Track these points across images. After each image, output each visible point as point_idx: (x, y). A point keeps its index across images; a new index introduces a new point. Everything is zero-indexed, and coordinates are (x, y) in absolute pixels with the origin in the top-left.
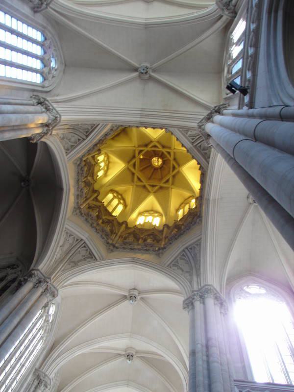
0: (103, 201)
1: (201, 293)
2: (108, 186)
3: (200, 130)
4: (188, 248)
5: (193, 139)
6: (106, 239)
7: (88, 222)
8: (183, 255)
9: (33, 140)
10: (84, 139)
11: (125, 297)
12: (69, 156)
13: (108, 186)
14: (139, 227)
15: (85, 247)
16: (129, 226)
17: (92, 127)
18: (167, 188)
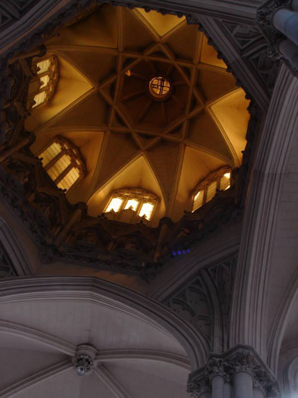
0: (40, 157)
1: (227, 361)
2: (52, 126)
3: (261, 22)
4: (209, 270)
5: (243, 43)
6: (40, 234)
7: (7, 195)
8: (198, 282)
10: (15, 19)
11: (66, 360)
13: (52, 126)
14: (110, 218)
16: (90, 213)
18: (176, 145)
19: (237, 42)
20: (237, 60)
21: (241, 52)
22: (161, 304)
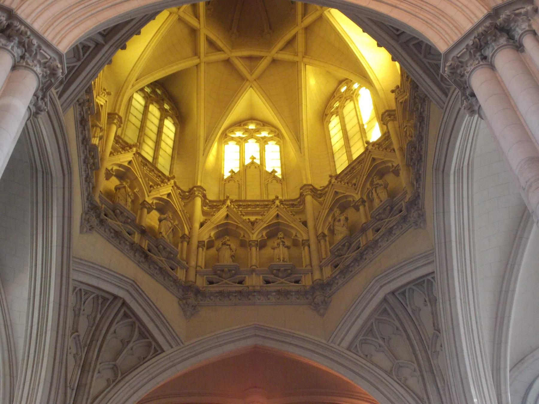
10: (124, 303)
12: (165, 346)
15: (404, 293)
22: (450, 95)
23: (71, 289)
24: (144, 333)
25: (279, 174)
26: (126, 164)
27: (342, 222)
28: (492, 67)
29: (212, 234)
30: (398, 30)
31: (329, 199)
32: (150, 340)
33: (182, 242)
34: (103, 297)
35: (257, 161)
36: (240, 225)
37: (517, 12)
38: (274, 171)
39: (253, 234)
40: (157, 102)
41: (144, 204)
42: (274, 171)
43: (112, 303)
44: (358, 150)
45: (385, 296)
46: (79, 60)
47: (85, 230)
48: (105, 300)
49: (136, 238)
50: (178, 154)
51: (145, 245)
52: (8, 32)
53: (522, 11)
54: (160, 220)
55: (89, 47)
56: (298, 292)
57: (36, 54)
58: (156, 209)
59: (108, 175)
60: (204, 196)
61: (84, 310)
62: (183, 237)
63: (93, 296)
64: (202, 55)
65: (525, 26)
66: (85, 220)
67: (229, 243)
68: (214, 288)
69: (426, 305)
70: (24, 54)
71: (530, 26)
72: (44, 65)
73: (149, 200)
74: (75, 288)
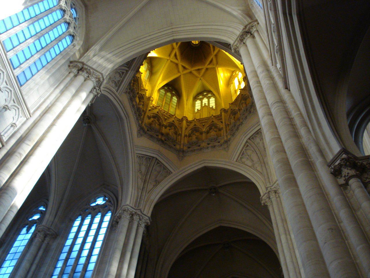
5: (123, 73)
9: (147, 223)
10: (156, 159)
17: (142, 157)
19: (124, 75)
20: (132, 71)
21: (127, 71)
23: (136, 157)
24: (165, 168)
25: (214, 107)
26: (156, 113)
27: (232, 118)
28: (246, 46)
29: (190, 132)
30: (227, 44)
31: (229, 112)
32: (167, 170)
33: (179, 136)
34: (148, 158)
35: (207, 105)
36: (200, 127)
37: (253, 25)
38: (213, 107)
39: (204, 129)
40: (170, 92)
41: (163, 125)
42: (213, 107)
43: (152, 160)
44: (238, 93)
45: (247, 141)
46: (121, 77)
47: (139, 136)
48: (150, 159)
49: (160, 137)
50: (178, 107)
51: (163, 138)
52: (82, 70)
53: (254, 25)
54: (169, 130)
55: (124, 72)
56: (218, 146)
57: (93, 75)
58: (168, 126)
59: (149, 118)
60: (187, 119)
61: (142, 163)
62: (179, 135)
63: (145, 158)
64: (181, 72)
65: (255, 29)
66: (139, 132)
67: (195, 134)
68: (190, 149)
69: (261, 141)
70: (89, 76)
71: (256, 29)
72: (96, 78)
73: (164, 123)
74: (137, 156)
